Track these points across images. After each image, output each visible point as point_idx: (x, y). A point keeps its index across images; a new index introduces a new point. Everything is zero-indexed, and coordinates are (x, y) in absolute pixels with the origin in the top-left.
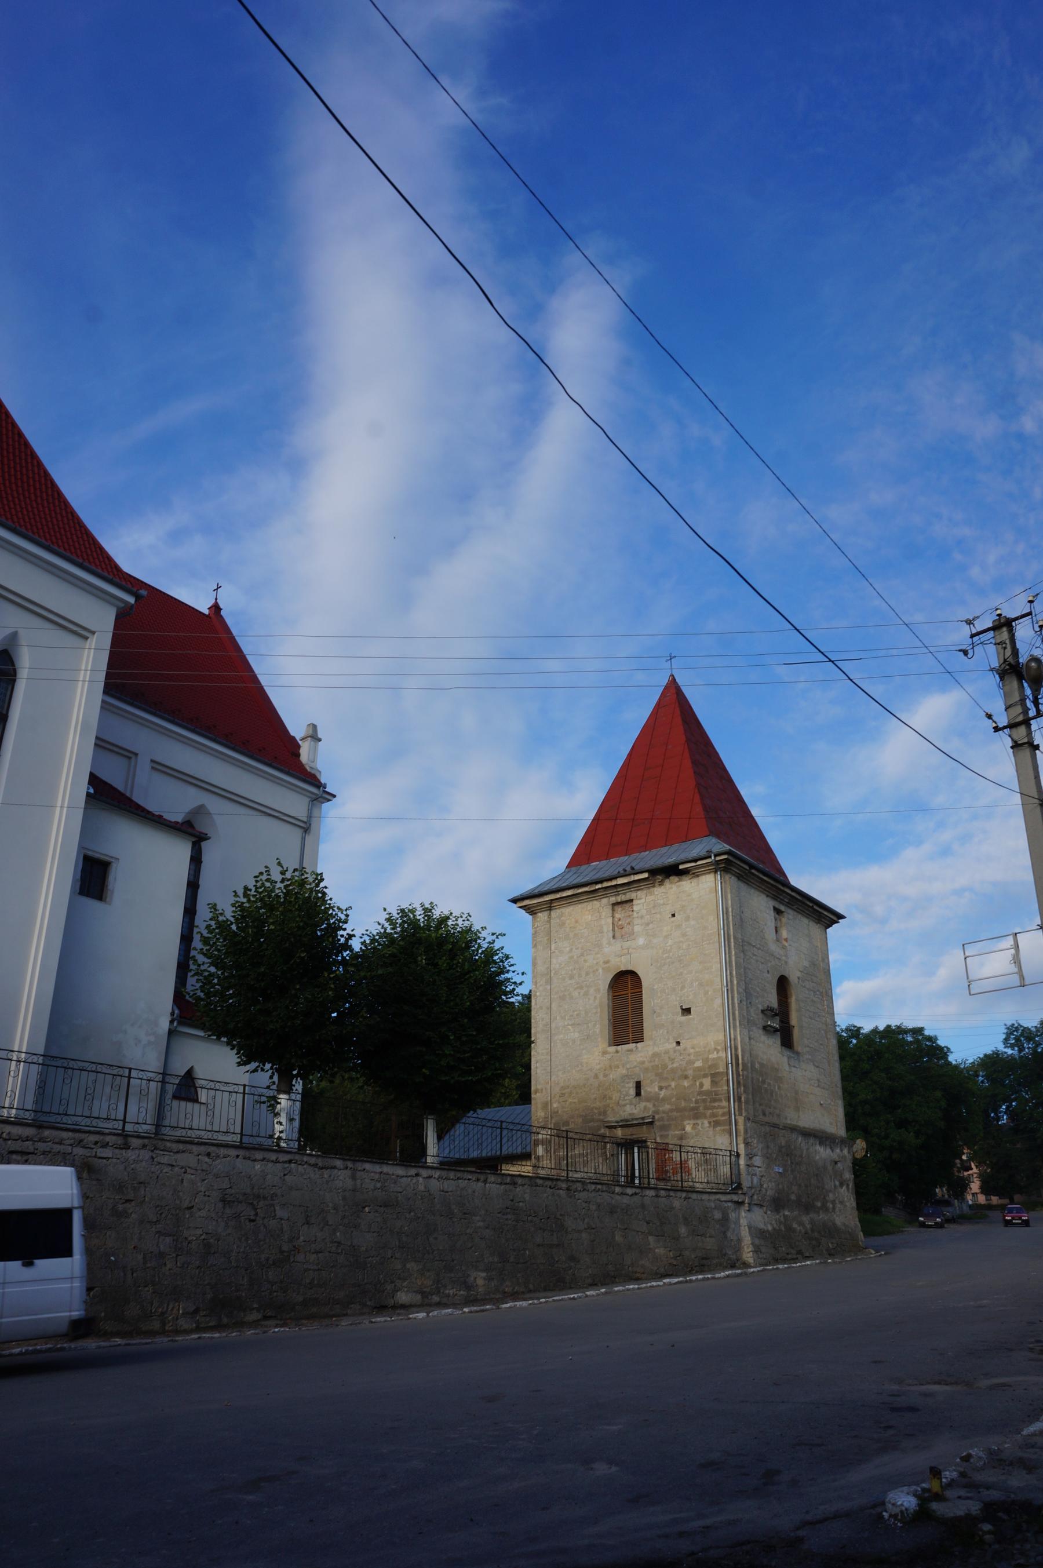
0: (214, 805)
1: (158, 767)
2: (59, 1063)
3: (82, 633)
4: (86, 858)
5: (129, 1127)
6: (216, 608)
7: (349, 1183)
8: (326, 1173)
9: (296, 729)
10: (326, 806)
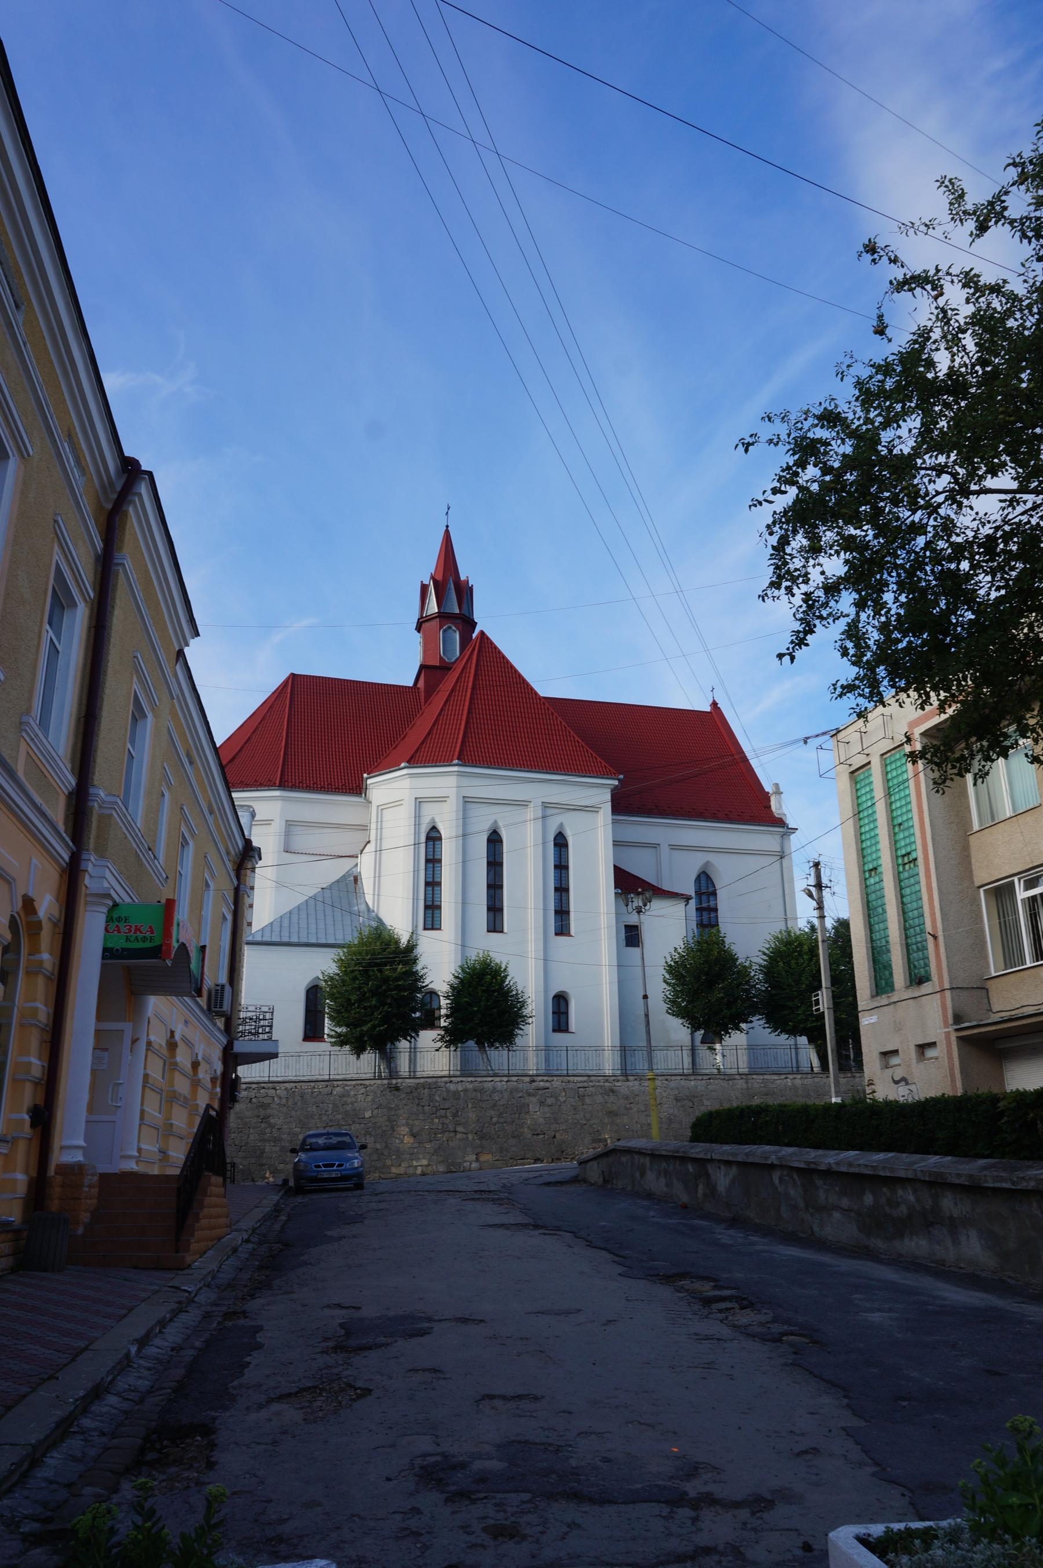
0: (716, 860)
1: (674, 847)
6: (714, 704)
7: (745, 1086)
8: (731, 1083)
9: (768, 788)
10: (792, 837)
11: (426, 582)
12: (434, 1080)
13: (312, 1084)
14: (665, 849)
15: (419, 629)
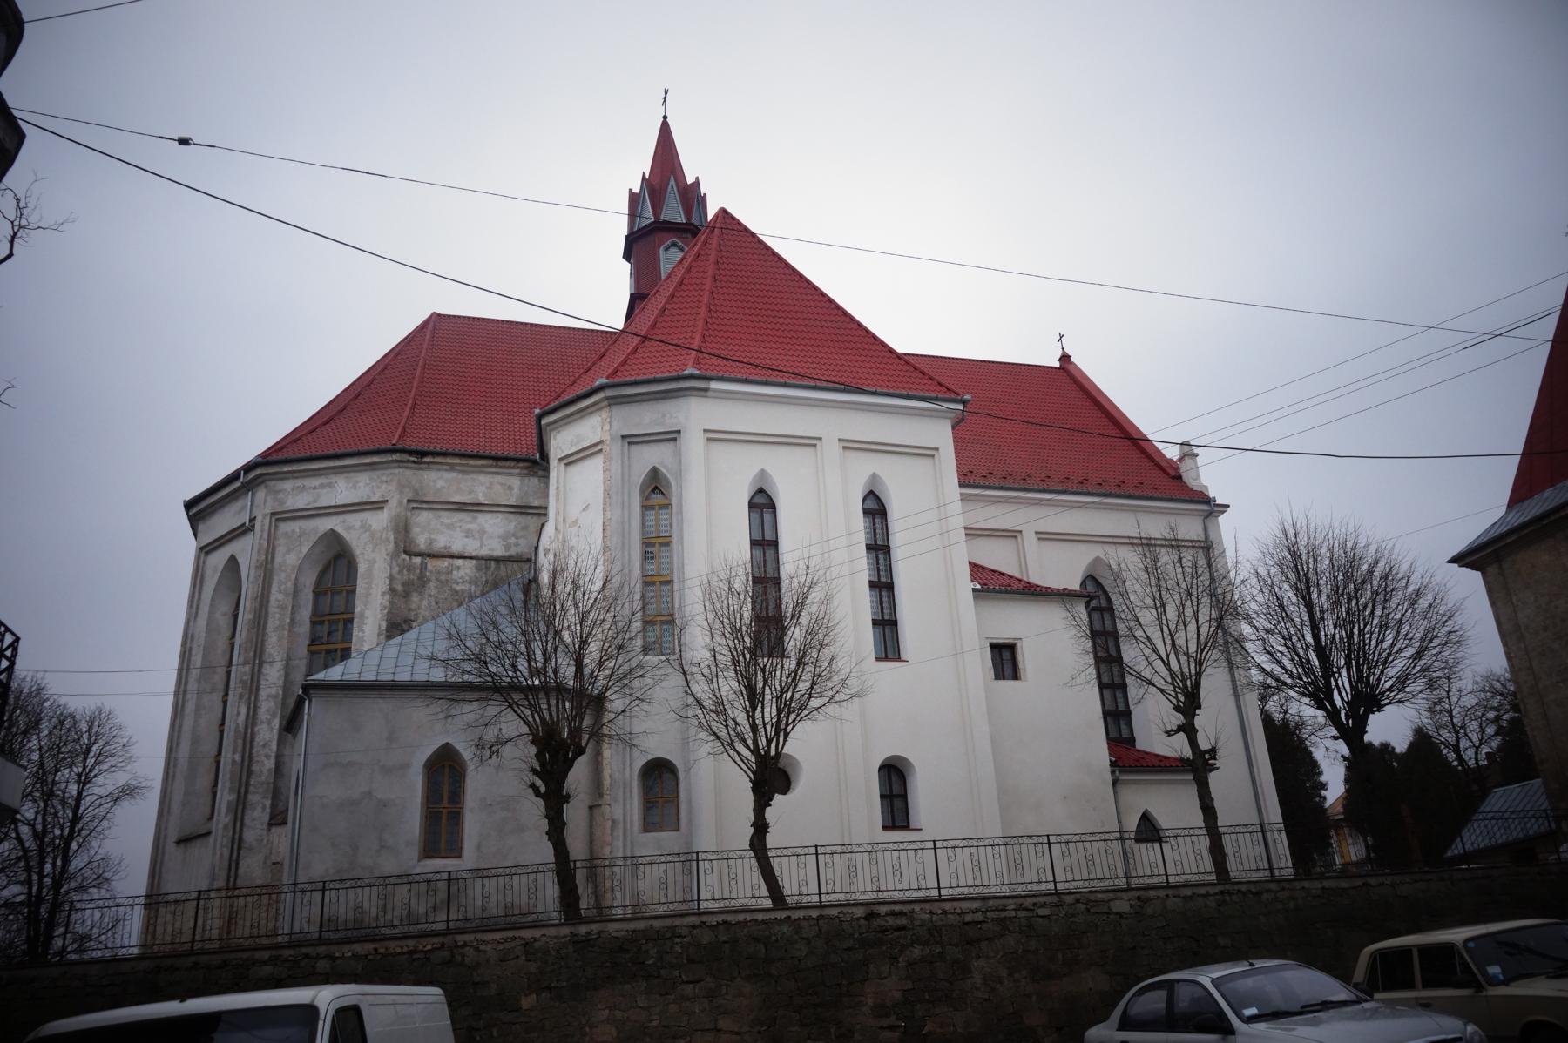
2: (986, 842)
3: (929, 453)
4: (993, 647)
5: (1060, 886)
6: (1065, 358)
9: (1172, 453)
10: (1222, 519)
11: (637, 190)
12: (668, 922)
13: (411, 943)
14: (1030, 540)
15: (627, 256)
